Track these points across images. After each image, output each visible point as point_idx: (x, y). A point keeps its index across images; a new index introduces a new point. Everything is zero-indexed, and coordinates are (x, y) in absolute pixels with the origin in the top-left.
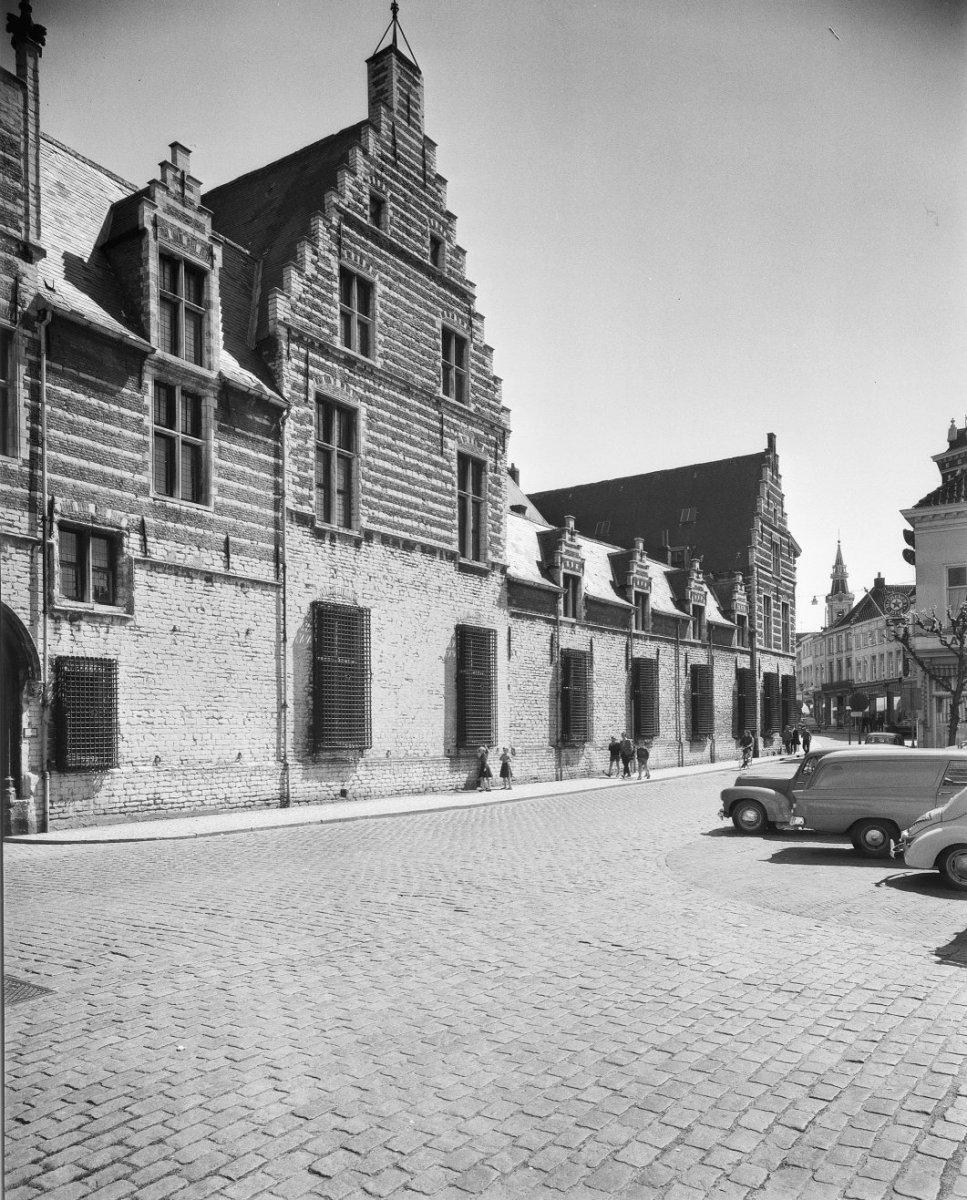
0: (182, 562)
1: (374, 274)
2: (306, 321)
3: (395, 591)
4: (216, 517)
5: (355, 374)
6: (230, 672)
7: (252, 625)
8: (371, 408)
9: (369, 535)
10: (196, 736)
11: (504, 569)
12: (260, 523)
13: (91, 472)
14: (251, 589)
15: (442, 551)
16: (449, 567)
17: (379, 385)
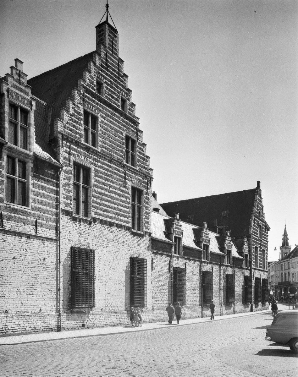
0: (17, 230)
2: (70, 132)
3: (105, 243)
4: (32, 212)
5: (89, 154)
6: (37, 276)
7: (46, 256)
8: (96, 168)
9: (95, 220)
10: (23, 302)
11: (150, 234)
12: (50, 214)
14: (46, 242)
15: (125, 226)
16: (128, 233)
17: (100, 158)
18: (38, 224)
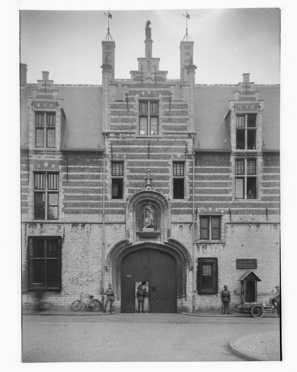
13: (210, 197)
18: (269, 212)
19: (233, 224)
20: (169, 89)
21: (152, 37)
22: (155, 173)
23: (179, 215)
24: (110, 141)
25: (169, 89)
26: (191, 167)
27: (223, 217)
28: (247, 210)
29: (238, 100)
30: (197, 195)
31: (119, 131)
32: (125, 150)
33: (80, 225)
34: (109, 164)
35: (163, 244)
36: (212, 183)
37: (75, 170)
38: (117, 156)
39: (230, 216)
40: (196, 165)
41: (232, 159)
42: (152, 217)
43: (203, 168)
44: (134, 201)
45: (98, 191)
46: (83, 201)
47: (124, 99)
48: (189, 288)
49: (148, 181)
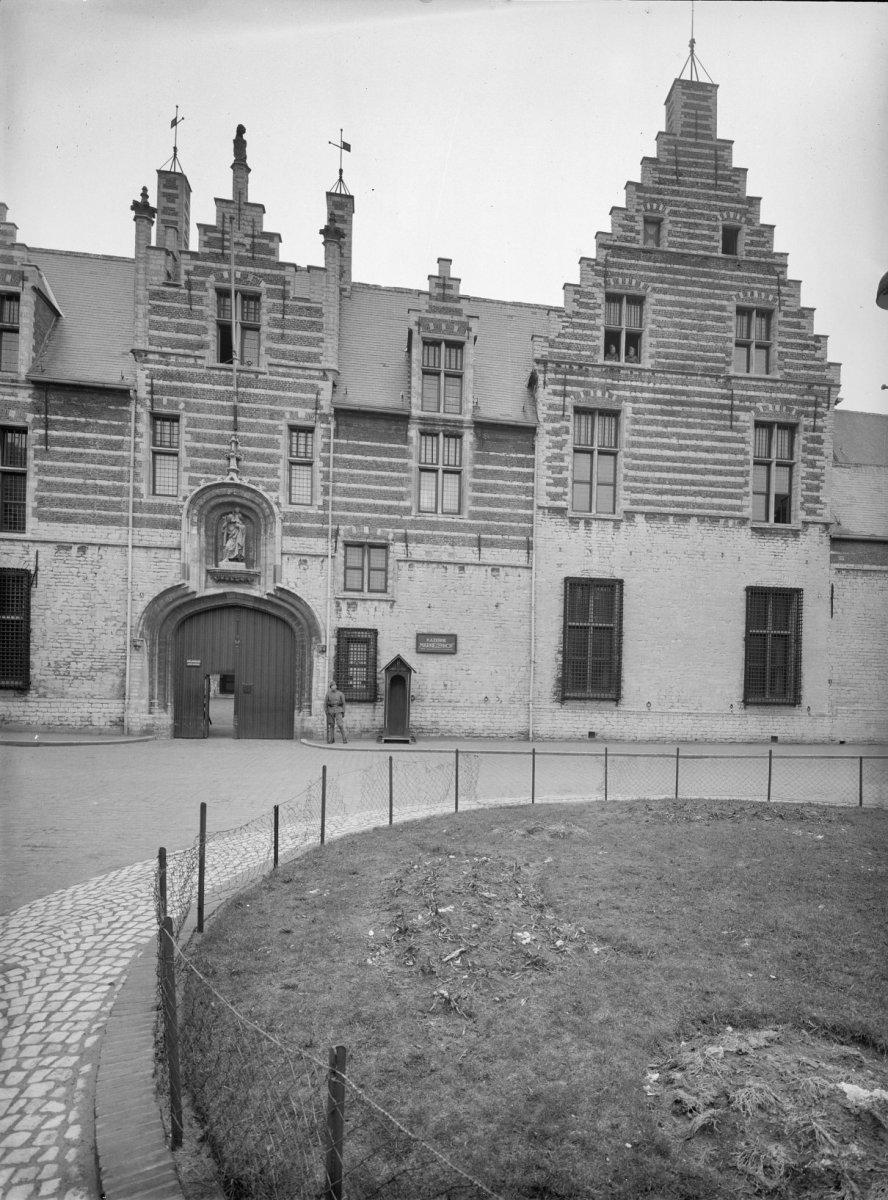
1: (646, 288)
8: (637, 405)
12: (512, 521)
13: (366, 505)
16: (745, 533)
18: (483, 543)
19: (411, 562)
20: (282, 273)
21: (248, 161)
22: (249, 446)
23: (300, 538)
24: (148, 369)
25: (282, 273)
26: (326, 440)
27: (391, 548)
28: (441, 536)
29: (427, 311)
30: (338, 499)
31: (169, 350)
32: (182, 392)
33: (75, 548)
34: (145, 418)
35: (265, 597)
36: (370, 476)
37: (64, 425)
38: (165, 402)
39: (407, 546)
40: (337, 436)
41: (413, 432)
42: (241, 540)
43: (353, 445)
44: (201, 502)
45: (119, 476)
46: (82, 496)
47: (182, 283)
48: (317, 689)
49: (233, 462)
